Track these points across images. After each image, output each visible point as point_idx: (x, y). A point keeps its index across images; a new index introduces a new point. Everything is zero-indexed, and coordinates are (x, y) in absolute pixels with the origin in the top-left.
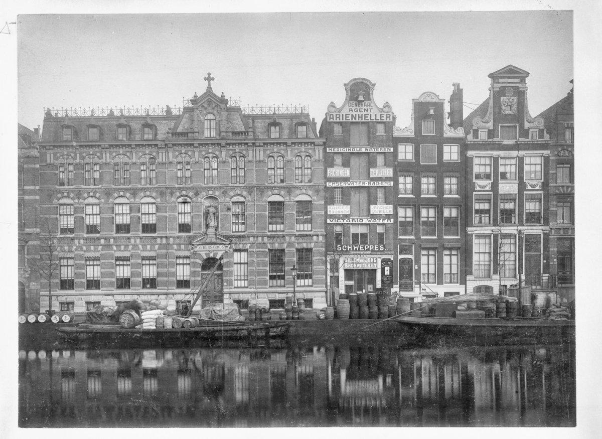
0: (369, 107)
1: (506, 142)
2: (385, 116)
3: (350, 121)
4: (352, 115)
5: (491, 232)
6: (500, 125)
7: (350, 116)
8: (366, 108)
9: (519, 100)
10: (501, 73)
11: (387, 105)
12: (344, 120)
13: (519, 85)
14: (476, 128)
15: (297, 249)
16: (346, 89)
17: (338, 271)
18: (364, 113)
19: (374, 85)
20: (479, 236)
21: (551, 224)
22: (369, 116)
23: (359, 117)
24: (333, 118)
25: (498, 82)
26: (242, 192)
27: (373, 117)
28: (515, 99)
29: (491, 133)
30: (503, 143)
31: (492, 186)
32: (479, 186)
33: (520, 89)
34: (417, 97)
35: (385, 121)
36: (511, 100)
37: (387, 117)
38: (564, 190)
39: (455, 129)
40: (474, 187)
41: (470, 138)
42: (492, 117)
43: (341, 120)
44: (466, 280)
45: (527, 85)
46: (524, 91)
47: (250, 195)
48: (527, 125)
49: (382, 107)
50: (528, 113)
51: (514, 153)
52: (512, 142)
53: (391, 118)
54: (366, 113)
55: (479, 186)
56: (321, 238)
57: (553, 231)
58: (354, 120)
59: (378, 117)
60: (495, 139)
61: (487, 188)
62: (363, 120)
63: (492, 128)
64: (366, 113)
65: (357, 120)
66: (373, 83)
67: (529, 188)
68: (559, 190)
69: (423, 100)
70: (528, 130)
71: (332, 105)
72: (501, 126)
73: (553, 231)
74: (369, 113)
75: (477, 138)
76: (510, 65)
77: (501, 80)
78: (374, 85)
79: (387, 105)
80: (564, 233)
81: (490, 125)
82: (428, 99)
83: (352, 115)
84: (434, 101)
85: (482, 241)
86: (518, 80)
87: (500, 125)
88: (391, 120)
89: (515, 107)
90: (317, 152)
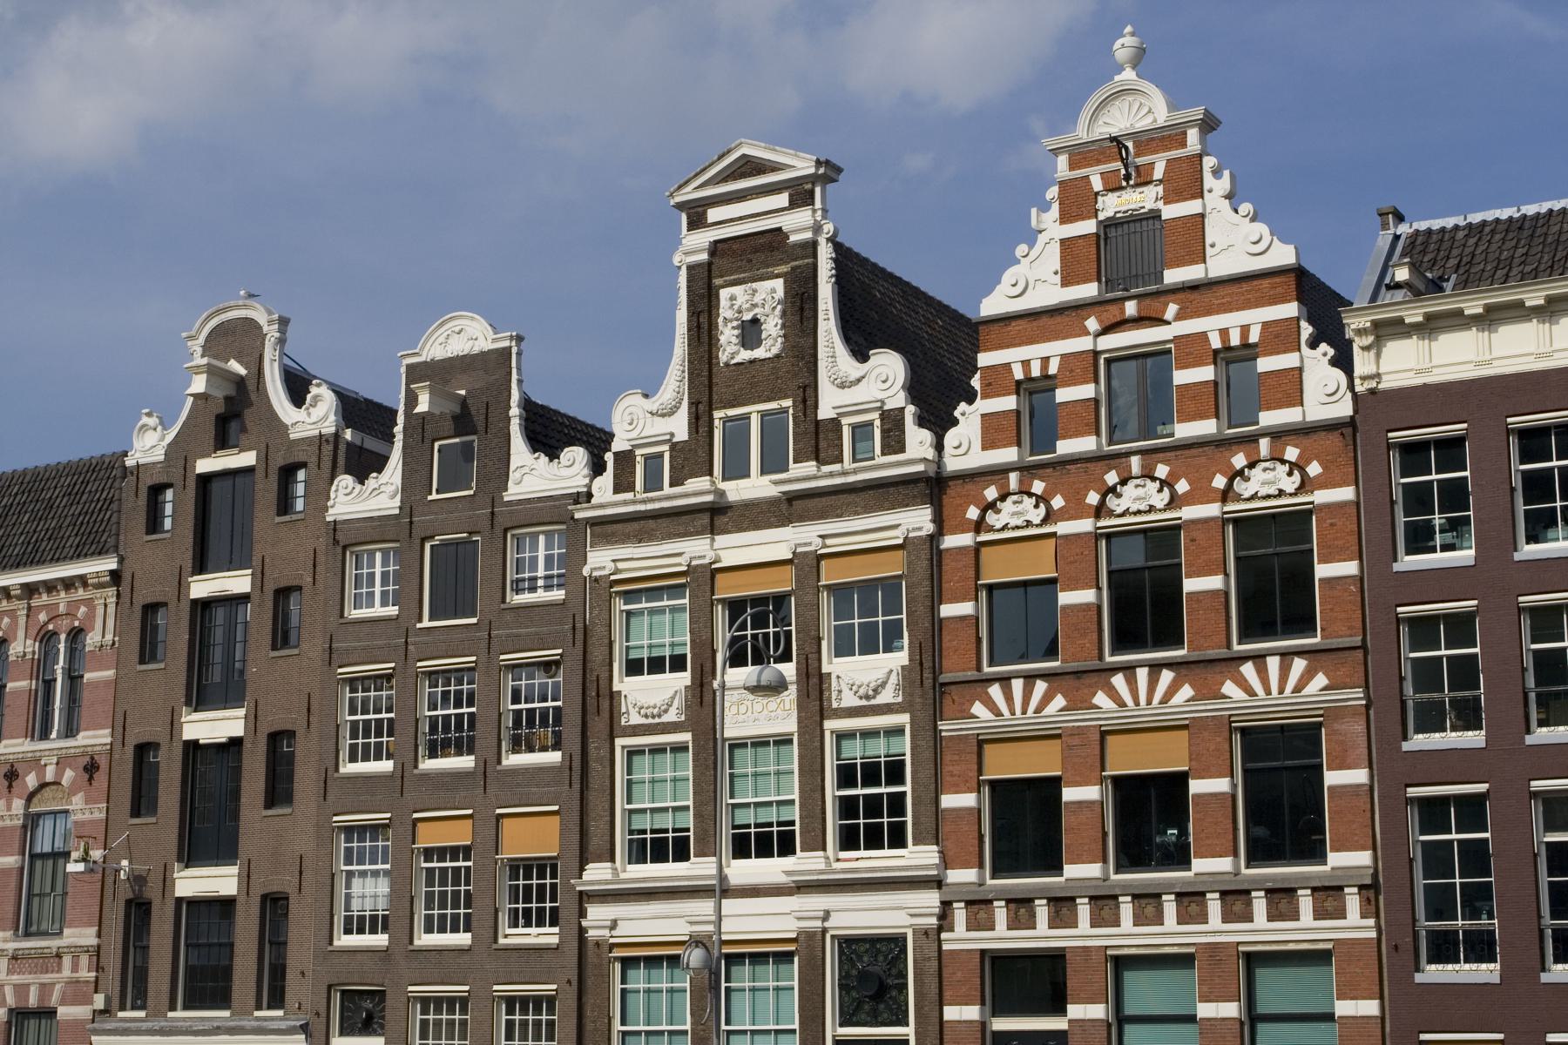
14: (626, 447)
36: (758, 299)
39: (553, 455)
57: (960, 914)
67: (850, 700)
70: (835, 424)
73: (960, 914)
77: (714, 214)
86: (782, 200)
90: (100, 611)
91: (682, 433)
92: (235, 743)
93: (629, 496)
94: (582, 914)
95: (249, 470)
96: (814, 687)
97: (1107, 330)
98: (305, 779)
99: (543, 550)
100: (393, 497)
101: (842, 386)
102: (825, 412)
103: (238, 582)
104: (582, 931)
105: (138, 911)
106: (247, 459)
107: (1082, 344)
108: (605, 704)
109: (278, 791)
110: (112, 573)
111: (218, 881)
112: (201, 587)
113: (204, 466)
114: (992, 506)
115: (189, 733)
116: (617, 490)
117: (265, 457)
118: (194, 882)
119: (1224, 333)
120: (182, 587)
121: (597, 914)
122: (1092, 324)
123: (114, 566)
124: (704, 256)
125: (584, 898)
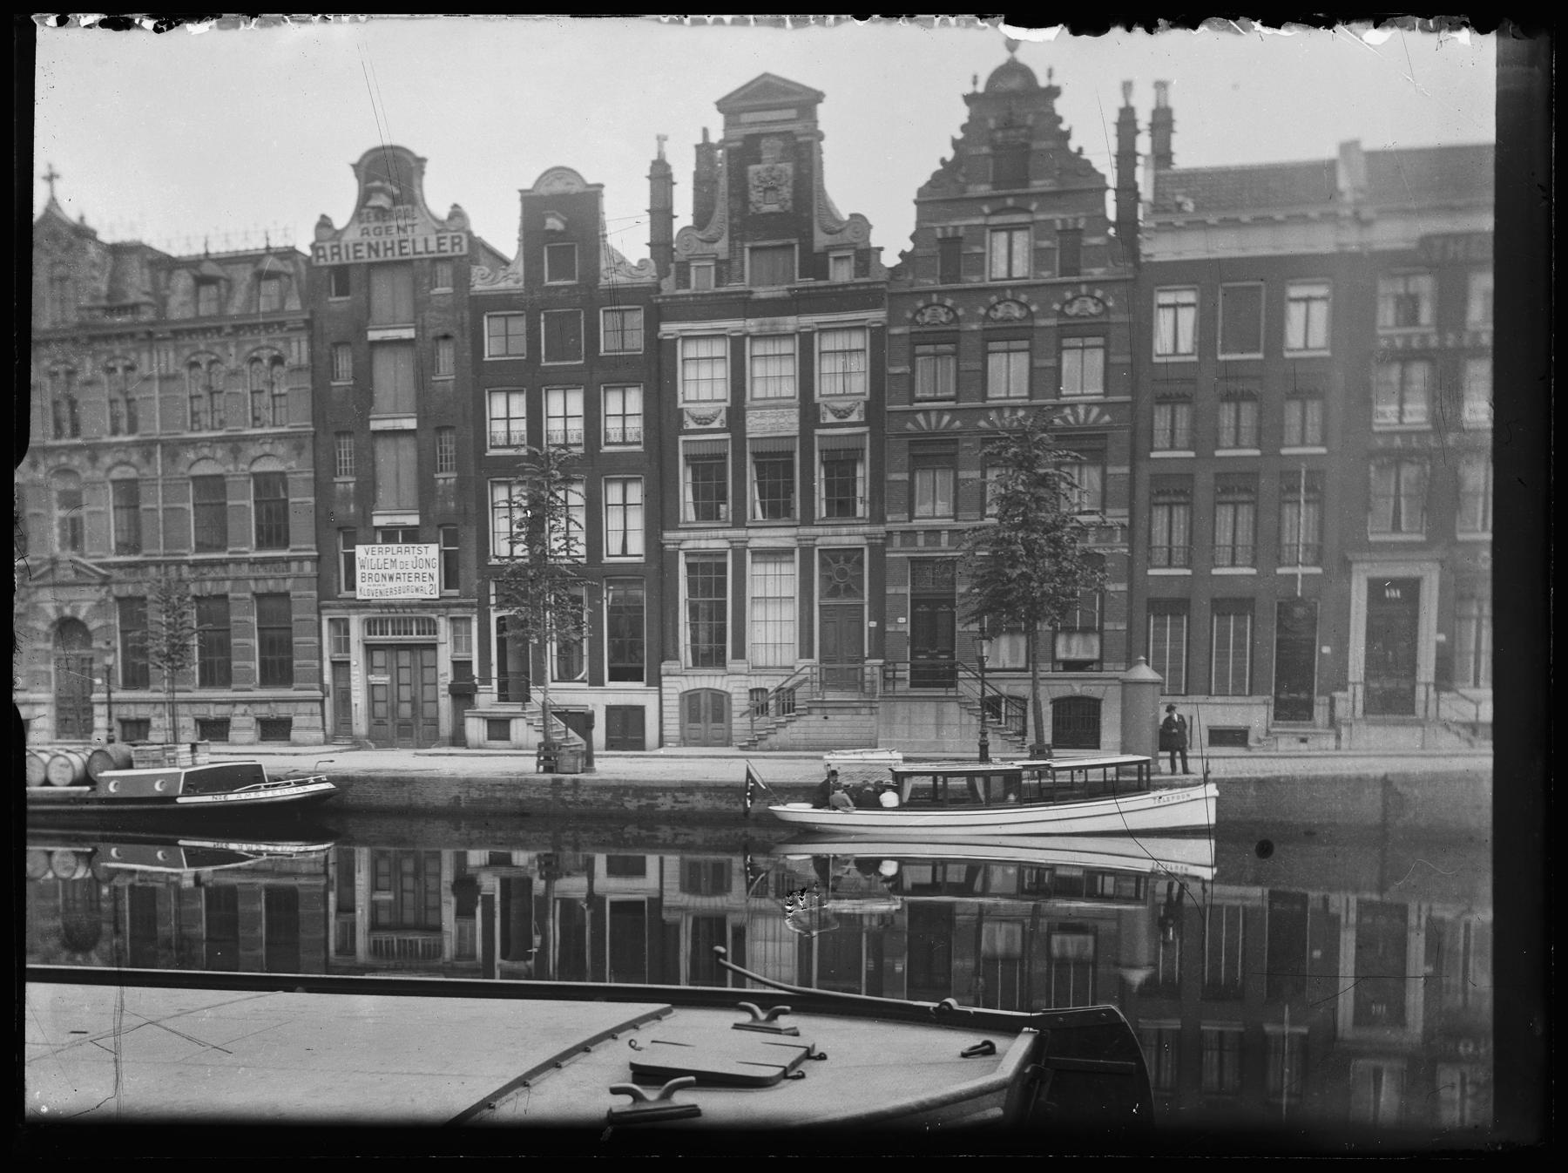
0: (409, 222)
1: (762, 293)
2: (448, 242)
3: (366, 260)
4: (370, 246)
5: (724, 544)
6: (748, 245)
7: (365, 248)
8: (401, 223)
9: (797, 169)
10: (745, 97)
11: (457, 213)
12: (352, 260)
13: (797, 127)
14: (683, 259)
15: (254, 594)
17: (348, 650)
18: (396, 238)
21: (889, 518)
22: (409, 245)
23: (386, 249)
24: (324, 256)
25: (740, 125)
27: (420, 247)
28: (788, 168)
29: (724, 269)
30: (755, 296)
33: (800, 139)
34: (528, 185)
35: (450, 254)
36: (775, 173)
37: (454, 244)
38: (928, 422)
40: (681, 421)
41: (668, 286)
42: (726, 228)
43: (345, 261)
44: (660, 677)
45: (821, 127)
46: (809, 144)
47: (148, 462)
48: (821, 240)
51: (790, 323)
52: (779, 291)
53: (465, 243)
54: (402, 236)
56: (308, 567)
58: (374, 258)
59: (433, 246)
61: (716, 425)
62: (397, 257)
63: (723, 256)
64: (402, 236)
65: (382, 258)
67: (830, 418)
68: (916, 422)
71: (324, 223)
72: (752, 250)
74: (409, 235)
75: (687, 284)
76: (765, 75)
79: (457, 213)
80: (927, 543)
81: (721, 247)
82: (559, 187)
83: (370, 246)
86: (792, 113)
87: (748, 245)
88: (465, 251)
89: (786, 192)
90: (294, 345)
97: (994, 213)
99: (637, 319)
100: (517, 282)
101: (830, 233)
107: (980, 221)
110: (306, 321)
114: (920, 311)
119: (1064, 221)
122: (986, 209)
124: (738, 144)
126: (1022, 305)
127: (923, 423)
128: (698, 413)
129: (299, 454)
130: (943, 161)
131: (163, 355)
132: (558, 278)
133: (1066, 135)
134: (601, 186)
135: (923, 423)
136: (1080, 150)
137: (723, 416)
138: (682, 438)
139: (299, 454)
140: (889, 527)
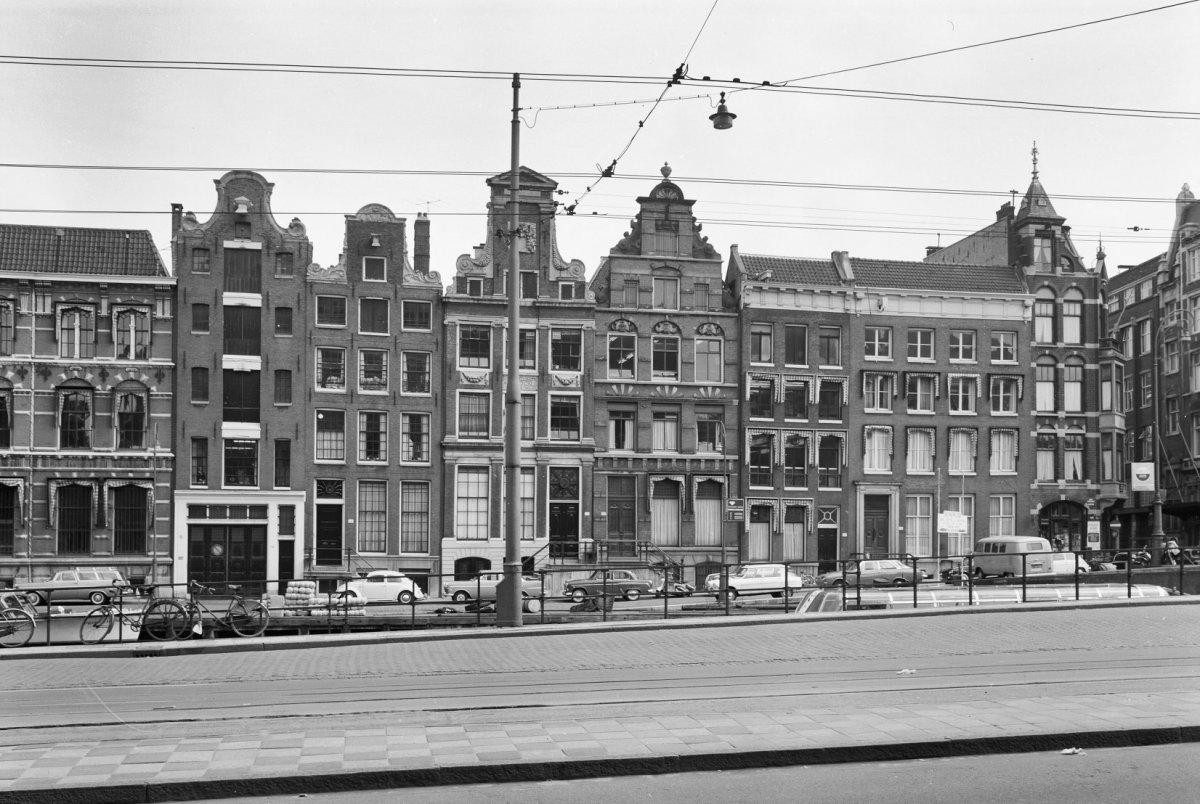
11: (296, 225)
16: (217, 189)
19: (273, 185)
20: (464, 469)
26: (140, 376)
31: (491, 380)
32: (466, 378)
34: (353, 210)
40: (459, 380)
47: (23, 378)
49: (286, 226)
50: (556, 253)
55: (466, 378)
60: (496, 296)
61: (482, 383)
66: (269, 181)
67: (558, 384)
69: (364, 218)
78: (273, 185)
79: (296, 225)
82: (375, 218)
84: (386, 219)
85: (473, 477)
86: (538, 194)
91: (488, 272)
92: (254, 374)
93: (461, 295)
94: (442, 454)
95: (258, 251)
96: (543, 376)
98: (297, 388)
102: (553, 275)
103: (254, 300)
104: (444, 460)
105: (201, 443)
106: (257, 246)
108: (454, 377)
109: (284, 392)
111: (247, 431)
112: (231, 299)
113: (228, 244)
115: (226, 365)
116: (458, 292)
117: (268, 246)
118: (234, 430)
120: (217, 298)
121: (448, 454)
123: (175, 283)
125: (443, 447)
126: (675, 325)
127: (616, 391)
128: (470, 376)
129: (159, 381)
130: (626, 234)
131: (40, 300)
132: (370, 278)
133: (700, 228)
134: (405, 220)
135: (616, 391)
136: (706, 239)
137: (487, 378)
138: (458, 391)
139: (159, 381)
140: (597, 455)
